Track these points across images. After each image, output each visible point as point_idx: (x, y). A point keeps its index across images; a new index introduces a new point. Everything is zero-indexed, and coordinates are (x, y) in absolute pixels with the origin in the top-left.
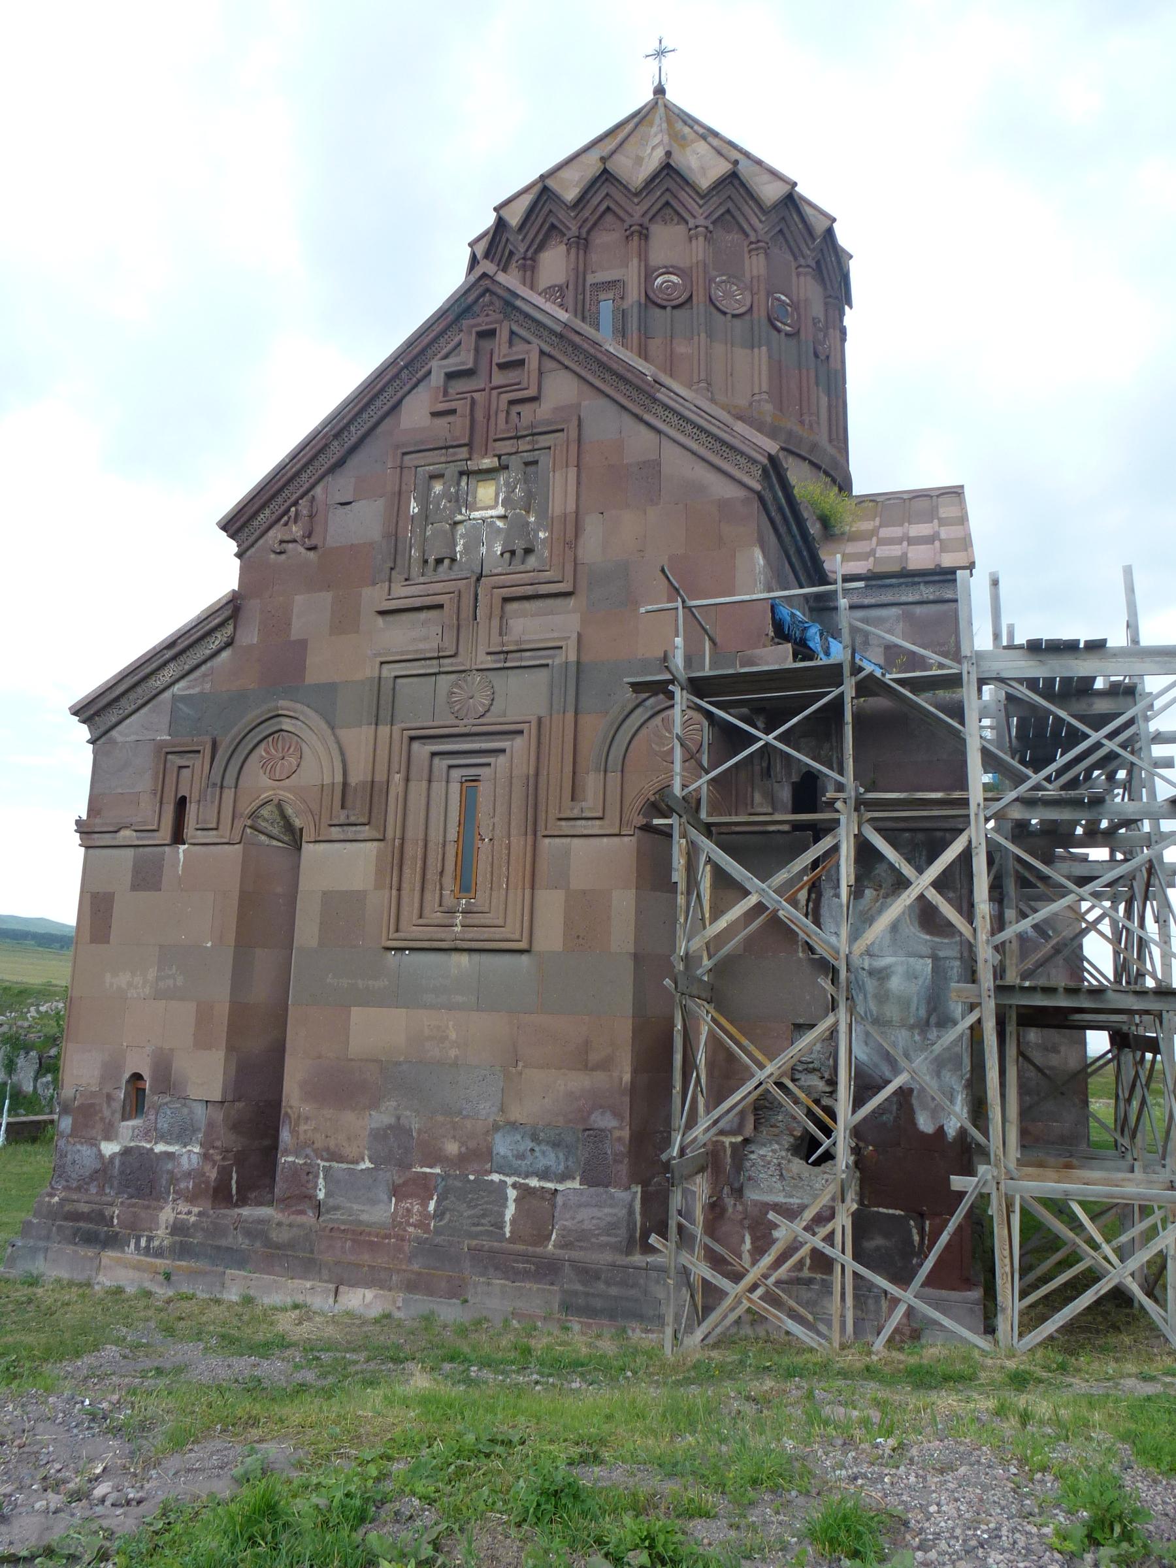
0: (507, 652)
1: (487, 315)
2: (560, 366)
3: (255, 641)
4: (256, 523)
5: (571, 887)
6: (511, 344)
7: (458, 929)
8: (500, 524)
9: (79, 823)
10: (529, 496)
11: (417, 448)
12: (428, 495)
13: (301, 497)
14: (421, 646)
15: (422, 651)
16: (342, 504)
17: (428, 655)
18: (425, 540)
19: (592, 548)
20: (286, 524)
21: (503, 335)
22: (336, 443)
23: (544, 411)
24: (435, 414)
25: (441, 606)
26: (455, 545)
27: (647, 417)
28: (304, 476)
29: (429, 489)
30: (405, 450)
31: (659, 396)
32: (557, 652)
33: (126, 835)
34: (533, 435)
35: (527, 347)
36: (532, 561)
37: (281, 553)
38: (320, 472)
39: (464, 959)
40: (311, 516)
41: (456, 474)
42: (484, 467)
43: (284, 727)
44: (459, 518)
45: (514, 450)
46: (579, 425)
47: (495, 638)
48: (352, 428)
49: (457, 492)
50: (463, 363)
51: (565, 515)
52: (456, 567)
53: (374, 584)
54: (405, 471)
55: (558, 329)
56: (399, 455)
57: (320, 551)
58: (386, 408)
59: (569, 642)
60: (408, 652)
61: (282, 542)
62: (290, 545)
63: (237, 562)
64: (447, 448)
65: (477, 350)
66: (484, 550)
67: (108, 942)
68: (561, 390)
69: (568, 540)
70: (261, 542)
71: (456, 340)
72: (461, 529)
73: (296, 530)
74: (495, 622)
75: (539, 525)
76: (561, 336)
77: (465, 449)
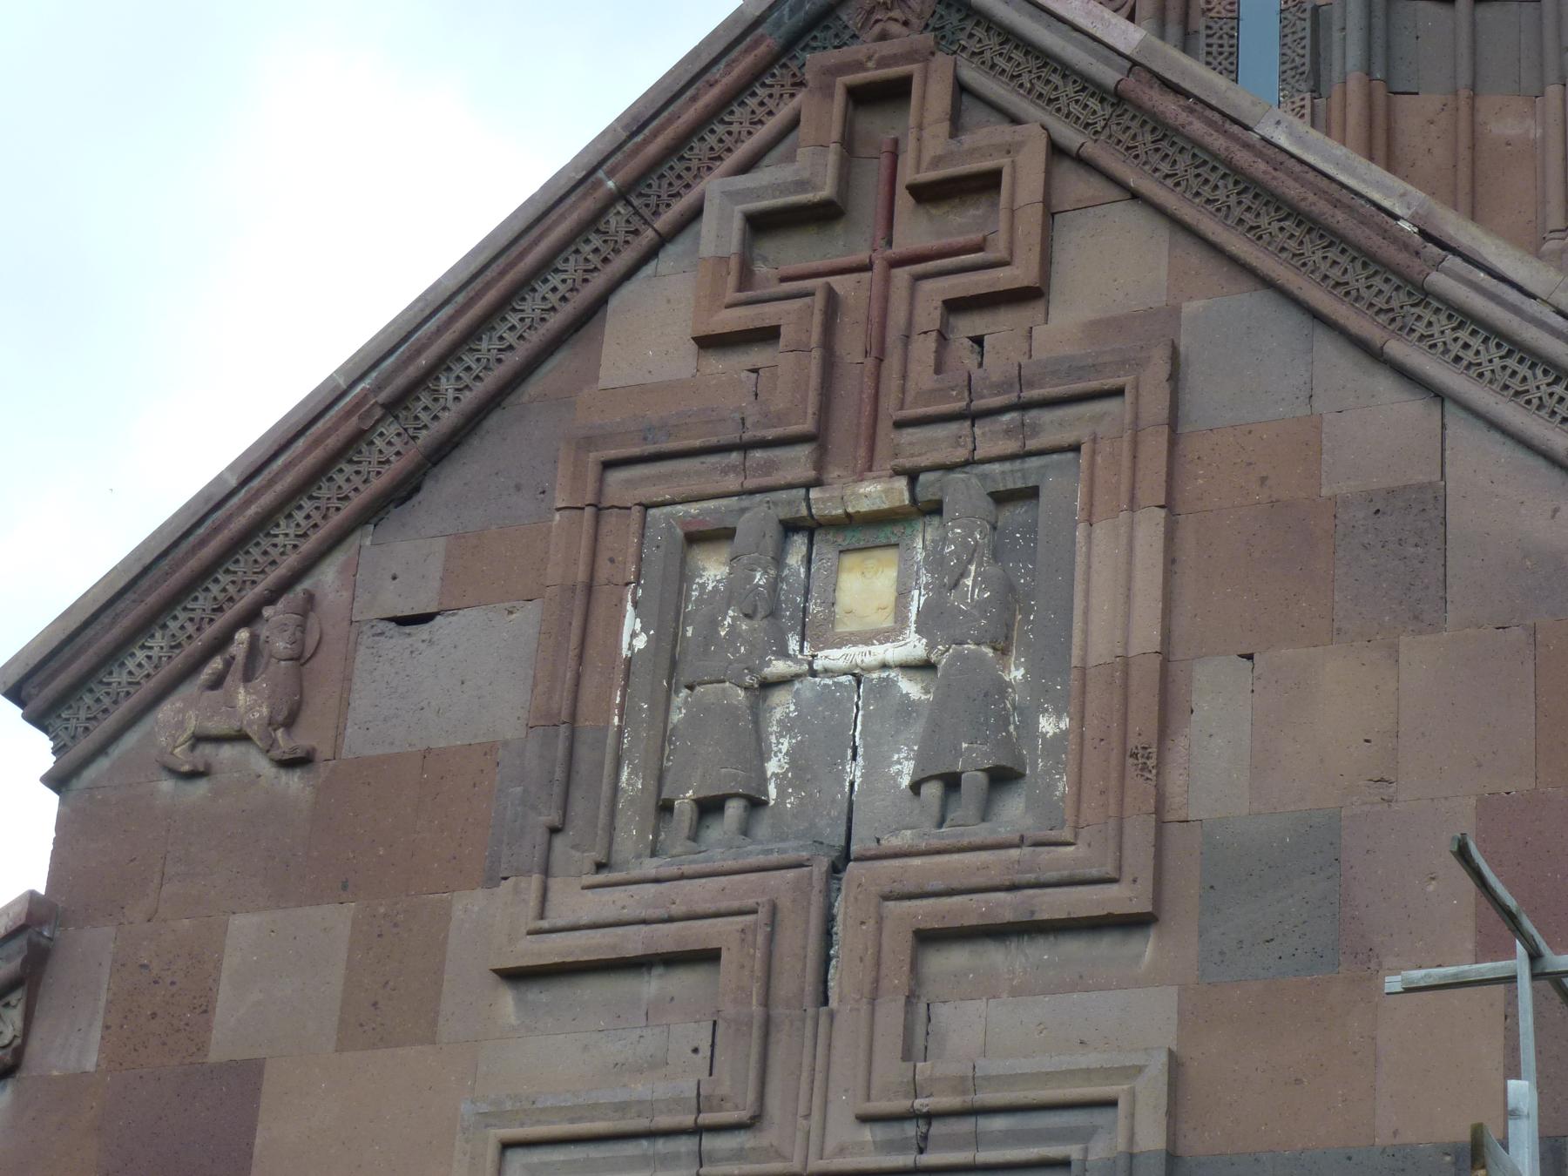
0: (930, 1117)
1: (883, 36)
2: (1115, 193)
3: (90, 1062)
4: (119, 678)
6: (956, 125)
8: (910, 688)
10: (1009, 598)
11: (650, 448)
12: (681, 595)
13: (272, 597)
14: (640, 1089)
17: (664, 1121)
18: (666, 736)
19: (1216, 764)
20: (217, 683)
21: (933, 96)
22: (391, 429)
23: (1060, 330)
24: (709, 343)
25: (710, 957)
26: (763, 755)
27: (1398, 349)
28: (285, 531)
29: (684, 575)
30: (613, 453)
31: (1438, 280)
32: (1099, 1117)
34: (1024, 406)
35: (1005, 132)
36: (1014, 811)
37: (194, 775)
38: (336, 519)
40: (299, 659)
41: (773, 531)
42: (864, 506)
44: (779, 667)
45: (960, 454)
46: (1174, 377)
47: (890, 1068)
48: (446, 384)
49: (774, 586)
50: (802, 185)
51: (1126, 661)
52: (764, 826)
53: (493, 879)
54: (611, 520)
55: (1109, 75)
56: (592, 471)
57: (322, 770)
58: (555, 321)
60: (594, 1110)
61: (199, 739)
62: (227, 752)
63: (52, 799)
64: (745, 447)
65: (848, 143)
69: (1133, 742)
70: (131, 739)
71: (784, 113)
72: (783, 705)
73: (248, 703)
74: (891, 1012)
75: (1041, 694)
76: (1118, 98)
77: (803, 452)
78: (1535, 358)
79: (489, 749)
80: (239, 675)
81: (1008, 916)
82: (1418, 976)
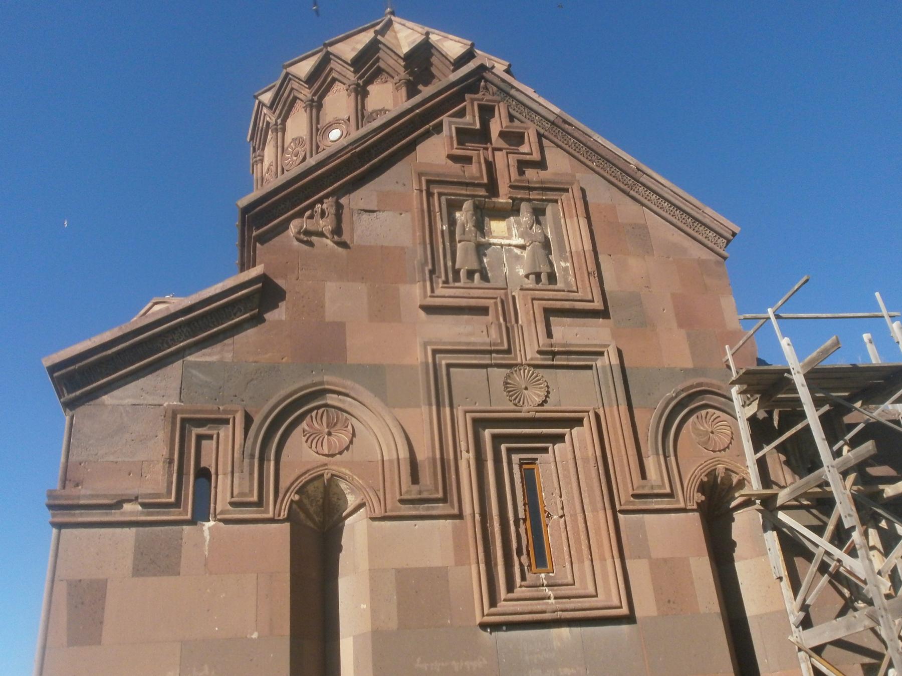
5: (654, 555)
9: (51, 495)
14: (472, 339)
15: (474, 344)
27: (632, 193)
33: (131, 509)
39: (565, 631)
43: (329, 402)
60: (459, 343)
66: (506, 269)
67: (99, 643)
68: (559, 163)
76: (553, 123)
78: (666, 200)
79: (402, 249)
81: (568, 307)
82: (748, 316)
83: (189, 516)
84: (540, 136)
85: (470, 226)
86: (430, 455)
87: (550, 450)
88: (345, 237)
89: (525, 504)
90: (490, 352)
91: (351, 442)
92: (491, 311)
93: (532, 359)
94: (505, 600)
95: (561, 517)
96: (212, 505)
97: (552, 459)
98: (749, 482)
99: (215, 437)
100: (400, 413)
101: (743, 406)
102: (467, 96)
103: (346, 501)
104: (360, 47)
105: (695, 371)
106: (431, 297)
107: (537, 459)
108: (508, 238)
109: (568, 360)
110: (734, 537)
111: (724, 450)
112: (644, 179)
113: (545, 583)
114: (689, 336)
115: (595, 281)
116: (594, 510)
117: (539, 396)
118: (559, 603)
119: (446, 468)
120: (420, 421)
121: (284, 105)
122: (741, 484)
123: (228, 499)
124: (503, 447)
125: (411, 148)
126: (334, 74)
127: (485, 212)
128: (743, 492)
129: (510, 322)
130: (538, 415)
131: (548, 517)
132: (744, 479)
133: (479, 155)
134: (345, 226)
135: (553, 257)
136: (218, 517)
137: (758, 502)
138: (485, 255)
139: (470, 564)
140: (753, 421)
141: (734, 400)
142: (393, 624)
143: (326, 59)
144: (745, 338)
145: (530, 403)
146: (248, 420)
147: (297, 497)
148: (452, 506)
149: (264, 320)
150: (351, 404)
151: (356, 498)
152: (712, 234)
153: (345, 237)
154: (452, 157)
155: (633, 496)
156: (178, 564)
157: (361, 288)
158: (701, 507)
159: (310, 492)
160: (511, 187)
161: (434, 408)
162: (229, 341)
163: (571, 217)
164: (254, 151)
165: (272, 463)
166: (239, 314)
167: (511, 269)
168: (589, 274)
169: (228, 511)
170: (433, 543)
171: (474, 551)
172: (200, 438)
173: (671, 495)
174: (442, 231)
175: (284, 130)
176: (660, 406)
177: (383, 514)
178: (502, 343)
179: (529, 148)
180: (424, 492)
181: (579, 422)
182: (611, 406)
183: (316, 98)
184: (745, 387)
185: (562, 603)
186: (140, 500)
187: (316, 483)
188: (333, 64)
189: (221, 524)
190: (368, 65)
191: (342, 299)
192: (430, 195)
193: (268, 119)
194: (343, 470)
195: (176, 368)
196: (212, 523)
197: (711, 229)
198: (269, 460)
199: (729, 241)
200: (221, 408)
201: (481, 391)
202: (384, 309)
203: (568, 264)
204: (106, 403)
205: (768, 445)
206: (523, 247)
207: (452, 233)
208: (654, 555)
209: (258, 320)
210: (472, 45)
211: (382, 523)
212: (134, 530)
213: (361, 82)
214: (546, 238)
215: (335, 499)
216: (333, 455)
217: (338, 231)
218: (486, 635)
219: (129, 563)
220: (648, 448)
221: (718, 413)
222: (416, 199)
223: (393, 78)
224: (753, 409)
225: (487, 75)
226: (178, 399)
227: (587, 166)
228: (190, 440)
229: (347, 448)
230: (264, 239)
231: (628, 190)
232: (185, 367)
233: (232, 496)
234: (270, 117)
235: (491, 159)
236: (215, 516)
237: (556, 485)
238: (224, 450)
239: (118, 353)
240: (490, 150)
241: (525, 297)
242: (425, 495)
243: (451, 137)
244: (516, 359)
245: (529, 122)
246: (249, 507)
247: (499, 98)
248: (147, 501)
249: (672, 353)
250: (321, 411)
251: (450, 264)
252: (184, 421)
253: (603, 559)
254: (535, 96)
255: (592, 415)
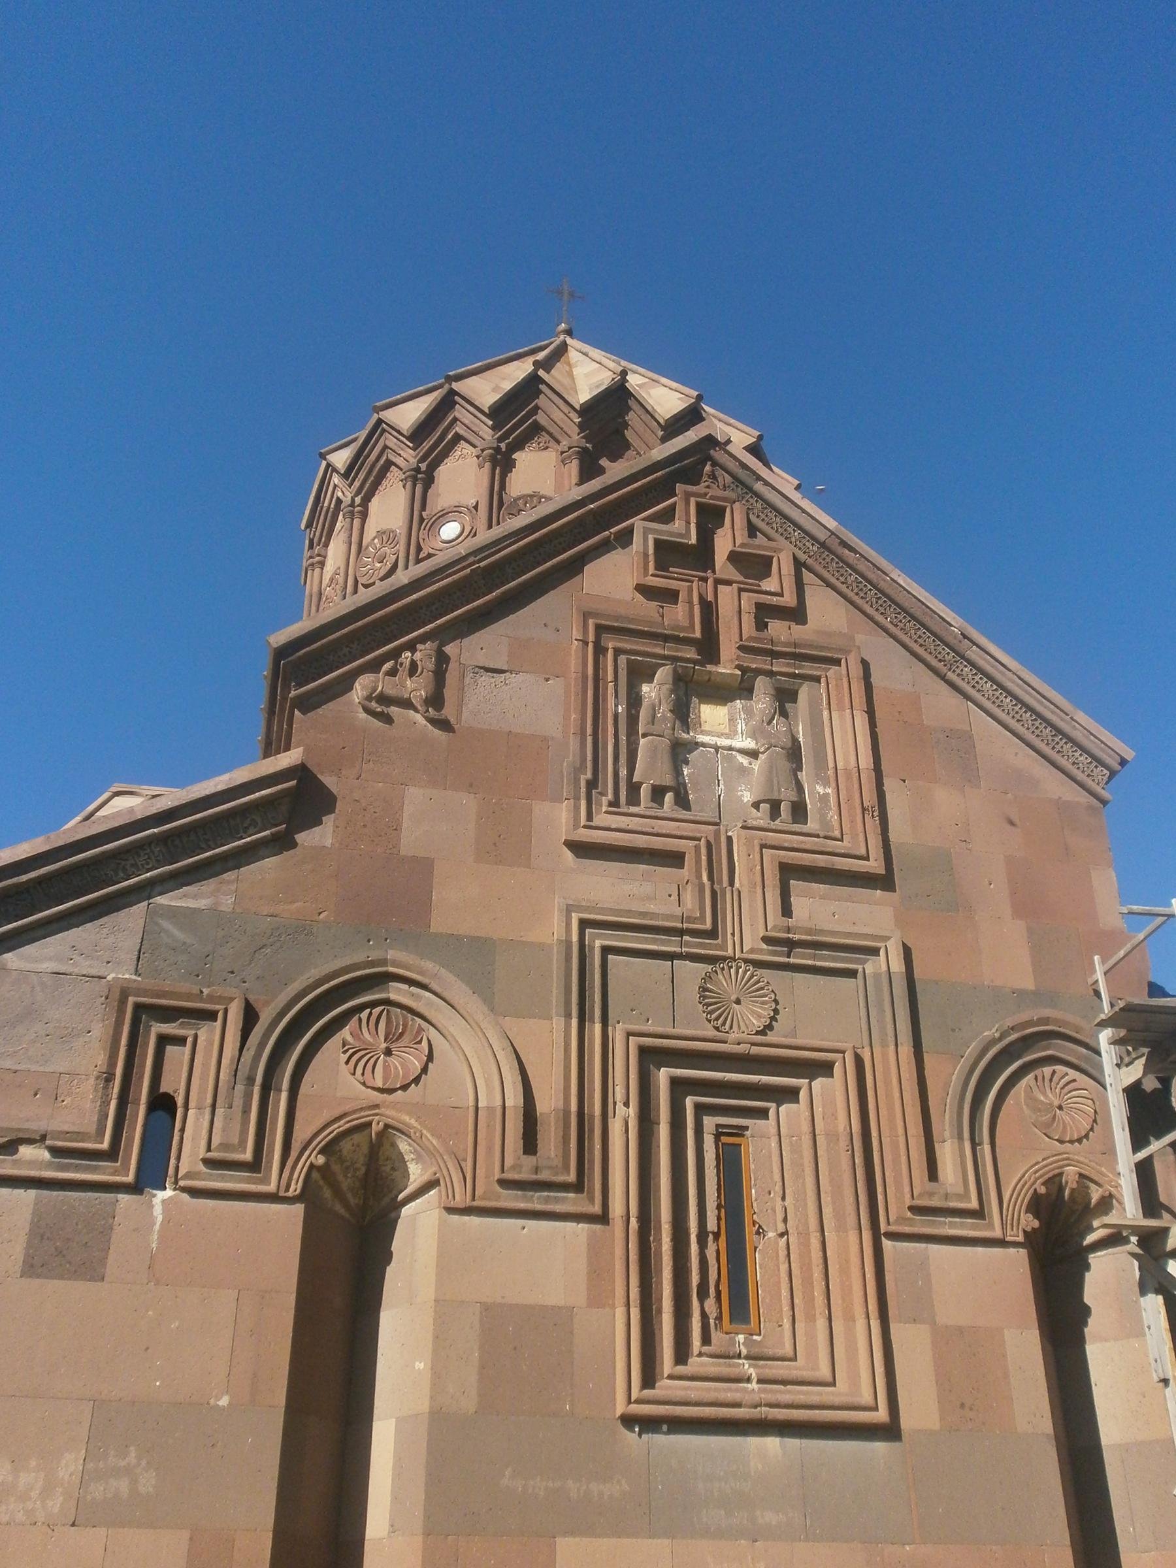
5: (942, 1320)
7: (754, 1385)
8: (743, 760)
14: (652, 907)
16: (488, 670)
20: (393, 673)
27: (950, 675)
31: (969, 654)
39: (772, 1443)
43: (393, 996)
59: (889, 944)
60: (629, 913)
68: (827, 614)
76: (823, 545)
78: (1009, 693)
79: (545, 739)
80: (406, 672)
81: (823, 865)
82: (1135, 908)
83: (130, 1178)
84: (799, 565)
85: (664, 711)
86: (561, 1104)
87: (772, 1113)
88: (448, 712)
89: (719, 1207)
90: (681, 932)
91: (425, 1070)
92: (689, 860)
93: (752, 951)
94: (670, 1377)
95: (782, 1235)
96: (173, 1161)
97: (774, 1131)
98: (1120, 1203)
99: (190, 1040)
100: (513, 1025)
101: (1118, 1065)
102: (680, 488)
103: (406, 1175)
104: (508, 386)
105: (1035, 997)
106: (585, 827)
107: (746, 1128)
108: (728, 736)
109: (814, 957)
110: (1088, 1299)
111: (1079, 1141)
112: (973, 653)
113: (744, 1351)
114: (1030, 931)
115: (873, 824)
116: (841, 1228)
117: (759, 1016)
118: (765, 1391)
119: (585, 1129)
120: (548, 1042)
121: (369, 473)
122: (1106, 1204)
123: (202, 1153)
124: (689, 1102)
125: (575, 567)
126: (459, 429)
127: (691, 690)
128: (1107, 1220)
129: (720, 882)
130: (755, 1050)
131: (758, 1233)
132: (1111, 1196)
133: (690, 589)
134: (449, 693)
135: (803, 776)
136: (182, 1183)
137: (1134, 1239)
138: (687, 762)
139: (613, 1307)
140: (1133, 1093)
141: (1104, 1054)
142: (469, 1404)
143: (448, 402)
144: (1129, 946)
145: (743, 1028)
146: (250, 1016)
147: (321, 1160)
148: (591, 1200)
149: (294, 845)
150: (430, 1004)
151: (424, 1169)
152: (1084, 759)
153: (448, 712)
154: (641, 589)
155: (911, 1208)
156: (103, 1261)
157: (467, 802)
158: (1031, 1241)
159: (345, 1152)
160: (741, 648)
161: (574, 1022)
162: (230, 876)
163: (841, 709)
164: (311, 547)
165: (284, 1096)
166: (251, 831)
167: (730, 789)
168: (864, 810)
169: (199, 1173)
170: (554, 1262)
171: (623, 1284)
172: (164, 1041)
173: (979, 1214)
174: (616, 715)
175: (364, 515)
176: (971, 1051)
177: (469, 1202)
178: (702, 918)
179: (778, 584)
180: (544, 1168)
181: (826, 1069)
182: (884, 1045)
183: (423, 466)
184: (1123, 1033)
185: (771, 1391)
186: (48, 1142)
187: (357, 1138)
188: (459, 412)
189: (185, 1196)
190: (517, 418)
191: (431, 819)
192: (600, 651)
193: (340, 494)
194: (406, 1118)
195: (134, 916)
196: (169, 1193)
197: (1084, 750)
198: (280, 1091)
199: (1113, 774)
200: (206, 991)
201: (656, 1000)
202: (504, 843)
203: (829, 790)
204: (10, 965)
205: (1158, 1137)
206: (753, 754)
207: (633, 720)
208: (942, 1320)
209: (283, 843)
210: (699, 398)
211: (466, 1218)
212: (32, 1193)
213: (503, 446)
214: (795, 740)
215: (388, 1169)
216: (391, 1091)
217: (436, 700)
218: (631, 1437)
219: (18, 1250)
220: (943, 1126)
221: (1073, 1074)
222: (574, 655)
223: (558, 442)
224: (1134, 1072)
225: (717, 454)
226: (133, 970)
227: (877, 623)
228: (147, 1044)
229: (417, 1080)
230: (307, 704)
231: (944, 670)
232: (152, 915)
233: (209, 1149)
234: (343, 491)
235: (710, 598)
236: (176, 1182)
237: (777, 1176)
238: (204, 1065)
239: (39, 881)
240: (710, 581)
241: (749, 841)
242: (545, 1176)
243: (646, 555)
244: (724, 947)
245: (782, 539)
246: (237, 1173)
247: (733, 495)
248: (60, 1144)
249: (1000, 960)
250: (379, 1009)
251: (623, 772)
252: (138, 1007)
253: (850, 1318)
254: (796, 496)
255: (849, 1057)
